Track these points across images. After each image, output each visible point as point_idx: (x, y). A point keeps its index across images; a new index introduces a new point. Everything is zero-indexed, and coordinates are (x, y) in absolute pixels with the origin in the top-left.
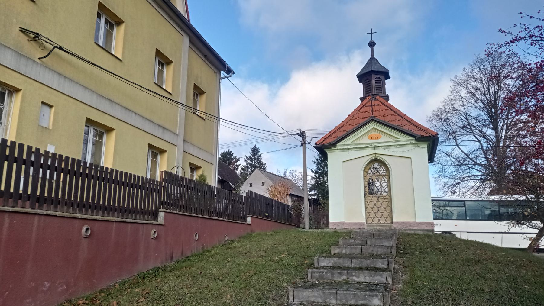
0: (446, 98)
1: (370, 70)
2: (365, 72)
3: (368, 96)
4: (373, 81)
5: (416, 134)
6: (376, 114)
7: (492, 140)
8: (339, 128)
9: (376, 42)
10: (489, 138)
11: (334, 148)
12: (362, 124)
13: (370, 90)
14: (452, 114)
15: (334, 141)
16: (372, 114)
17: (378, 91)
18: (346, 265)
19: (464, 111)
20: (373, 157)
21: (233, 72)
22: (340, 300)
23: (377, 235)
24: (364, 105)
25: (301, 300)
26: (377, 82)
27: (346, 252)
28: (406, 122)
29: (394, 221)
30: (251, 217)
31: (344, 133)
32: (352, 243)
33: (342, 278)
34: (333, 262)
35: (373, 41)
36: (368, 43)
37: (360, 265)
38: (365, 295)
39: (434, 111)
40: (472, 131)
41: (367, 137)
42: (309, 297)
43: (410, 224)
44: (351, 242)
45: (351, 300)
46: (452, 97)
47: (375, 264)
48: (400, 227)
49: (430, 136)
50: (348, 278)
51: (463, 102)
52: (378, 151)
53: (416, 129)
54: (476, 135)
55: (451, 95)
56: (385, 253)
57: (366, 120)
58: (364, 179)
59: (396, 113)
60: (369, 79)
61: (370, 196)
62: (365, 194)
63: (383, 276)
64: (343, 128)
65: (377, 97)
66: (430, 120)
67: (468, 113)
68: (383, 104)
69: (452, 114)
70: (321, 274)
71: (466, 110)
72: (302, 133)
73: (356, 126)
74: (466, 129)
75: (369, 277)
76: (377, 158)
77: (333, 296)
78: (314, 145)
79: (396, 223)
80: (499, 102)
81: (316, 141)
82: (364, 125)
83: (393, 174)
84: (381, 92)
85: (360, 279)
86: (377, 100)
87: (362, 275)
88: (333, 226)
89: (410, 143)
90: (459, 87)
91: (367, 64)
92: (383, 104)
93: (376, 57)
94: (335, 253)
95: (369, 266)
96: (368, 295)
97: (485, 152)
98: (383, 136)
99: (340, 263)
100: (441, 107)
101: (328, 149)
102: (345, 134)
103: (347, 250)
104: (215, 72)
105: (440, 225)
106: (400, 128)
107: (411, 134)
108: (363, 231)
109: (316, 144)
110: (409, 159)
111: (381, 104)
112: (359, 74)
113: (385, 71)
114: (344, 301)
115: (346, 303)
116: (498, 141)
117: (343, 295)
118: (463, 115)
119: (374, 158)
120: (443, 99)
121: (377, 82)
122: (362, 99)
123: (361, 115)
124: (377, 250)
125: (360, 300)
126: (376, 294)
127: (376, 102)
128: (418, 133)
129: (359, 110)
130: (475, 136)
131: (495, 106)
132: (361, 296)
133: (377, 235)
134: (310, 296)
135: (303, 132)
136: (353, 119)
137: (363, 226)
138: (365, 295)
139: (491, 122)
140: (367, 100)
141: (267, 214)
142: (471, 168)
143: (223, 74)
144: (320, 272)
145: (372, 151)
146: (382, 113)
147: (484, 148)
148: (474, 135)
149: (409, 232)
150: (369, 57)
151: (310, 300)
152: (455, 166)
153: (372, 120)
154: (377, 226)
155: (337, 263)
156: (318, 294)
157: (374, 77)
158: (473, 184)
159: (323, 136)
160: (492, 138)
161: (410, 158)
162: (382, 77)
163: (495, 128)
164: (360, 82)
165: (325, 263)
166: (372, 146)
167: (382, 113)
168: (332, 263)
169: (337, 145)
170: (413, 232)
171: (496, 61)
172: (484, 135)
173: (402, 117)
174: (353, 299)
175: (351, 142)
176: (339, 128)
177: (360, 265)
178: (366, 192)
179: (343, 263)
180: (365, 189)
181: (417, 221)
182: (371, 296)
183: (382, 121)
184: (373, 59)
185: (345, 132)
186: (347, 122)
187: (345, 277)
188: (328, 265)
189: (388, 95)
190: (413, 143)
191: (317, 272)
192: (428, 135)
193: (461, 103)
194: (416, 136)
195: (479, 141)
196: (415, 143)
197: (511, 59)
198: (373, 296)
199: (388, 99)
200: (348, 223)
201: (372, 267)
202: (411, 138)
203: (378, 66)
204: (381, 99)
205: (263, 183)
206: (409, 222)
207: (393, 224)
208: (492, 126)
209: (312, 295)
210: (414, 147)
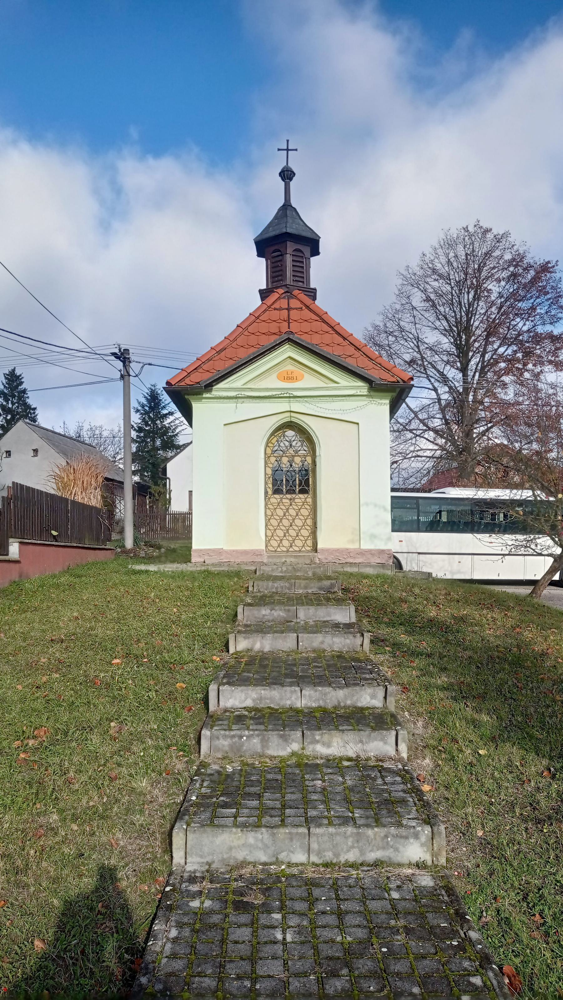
0: (388, 307)
1: (284, 230)
2: (272, 234)
3: (277, 288)
4: (288, 256)
5: (372, 376)
6: (294, 327)
7: (456, 388)
8: (219, 350)
9: (295, 171)
10: (452, 385)
11: (208, 395)
12: (267, 347)
13: (281, 275)
14: (396, 337)
15: (208, 380)
16: (289, 328)
17: (297, 279)
18: (288, 702)
19: (415, 333)
20: (285, 418)
22: (319, 853)
23: (302, 585)
24: (269, 307)
25: (209, 859)
26: (295, 259)
27: (262, 646)
28: (352, 350)
29: (319, 546)
30: (20, 543)
31: (229, 365)
32: (266, 617)
33: (289, 750)
34: (254, 695)
35: (291, 169)
36: (279, 171)
37: (322, 703)
38: (386, 836)
39: (367, 329)
40: (425, 369)
41: (275, 376)
42: (231, 849)
43: (349, 553)
44: (264, 615)
45: (348, 851)
46: (398, 307)
47: (355, 698)
48: (331, 558)
49: (398, 382)
50: (303, 749)
51: (414, 317)
52: (296, 406)
53: (370, 364)
54: (433, 380)
55: (396, 301)
56: (349, 648)
57: (273, 339)
58: (266, 463)
59: (332, 327)
60: (279, 251)
61: (276, 496)
62: (266, 493)
63: (389, 741)
64: (229, 353)
65: (296, 292)
67: (420, 337)
68: (307, 307)
69: (396, 337)
70: (237, 739)
71: (418, 331)
72: (122, 354)
73: (252, 350)
74: (415, 366)
75: (356, 743)
76: (293, 420)
77: (298, 844)
78: (165, 386)
79: (323, 550)
80: (474, 321)
81: (168, 378)
83: (322, 455)
84: (303, 282)
85: (333, 748)
86: (296, 297)
87: (340, 740)
88: (200, 556)
89: (359, 393)
90: (410, 288)
91: (276, 217)
92: (307, 307)
93: (294, 203)
94: (238, 649)
95: (342, 704)
96: (393, 836)
97: (442, 410)
98: (306, 375)
99: (272, 699)
100: (378, 323)
101: (194, 395)
102: (232, 366)
103: (264, 641)
106: (342, 360)
107: (363, 374)
108: (263, 570)
109: (168, 383)
110: (356, 425)
111: (304, 308)
112: (258, 239)
113: (315, 237)
114: (329, 856)
115: (334, 861)
116: (466, 391)
117: (326, 838)
118: (413, 340)
119: (288, 420)
120: (381, 309)
121: (295, 259)
122: (264, 294)
123: (264, 327)
124: (331, 642)
125: (371, 851)
126: (414, 833)
127: (294, 303)
128: (376, 374)
129: (259, 316)
130: (430, 381)
131: (467, 329)
132: (375, 839)
133: (302, 585)
134: (235, 847)
135: (124, 350)
136: (246, 333)
137: (259, 557)
138: (386, 836)
139: (458, 356)
140: (274, 297)
141: (54, 533)
142: (419, 436)
144: (233, 736)
145: (283, 406)
146: (306, 327)
147: (443, 403)
148: (428, 377)
149: (349, 569)
150: (282, 202)
151: (235, 858)
152: (394, 431)
153: (289, 340)
154: (286, 557)
155: (265, 698)
156: (256, 839)
157: (291, 247)
158: (420, 465)
159: (184, 366)
160: (457, 385)
161: (358, 424)
162: (307, 250)
163: (464, 370)
164: (260, 254)
165: (235, 699)
166: (285, 395)
167: (306, 327)
168: (254, 700)
169: (214, 388)
170: (355, 570)
171: (476, 245)
172: (445, 380)
173: (345, 339)
174: (353, 847)
175: (244, 385)
176: (219, 352)
177: (321, 702)
178: (268, 490)
179: (281, 699)
180: (266, 483)
181: (363, 547)
182: (401, 837)
183: (308, 344)
184: (289, 207)
185: (231, 362)
186: (235, 339)
187: (295, 747)
188: (244, 705)
189: (315, 289)
190: (365, 393)
191: (225, 737)
192: (394, 380)
193: (412, 319)
194: (372, 379)
195: (435, 390)
197: (501, 244)
198: (406, 838)
199: (314, 298)
200: (230, 551)
201: (349, 707)
202: (360, 383)
203: (299, 224)
204: (302, 296)
205: (36, 451)
207: (316, 552)
208: (459, 364)
209: (242, 842)
210: (366, 402)
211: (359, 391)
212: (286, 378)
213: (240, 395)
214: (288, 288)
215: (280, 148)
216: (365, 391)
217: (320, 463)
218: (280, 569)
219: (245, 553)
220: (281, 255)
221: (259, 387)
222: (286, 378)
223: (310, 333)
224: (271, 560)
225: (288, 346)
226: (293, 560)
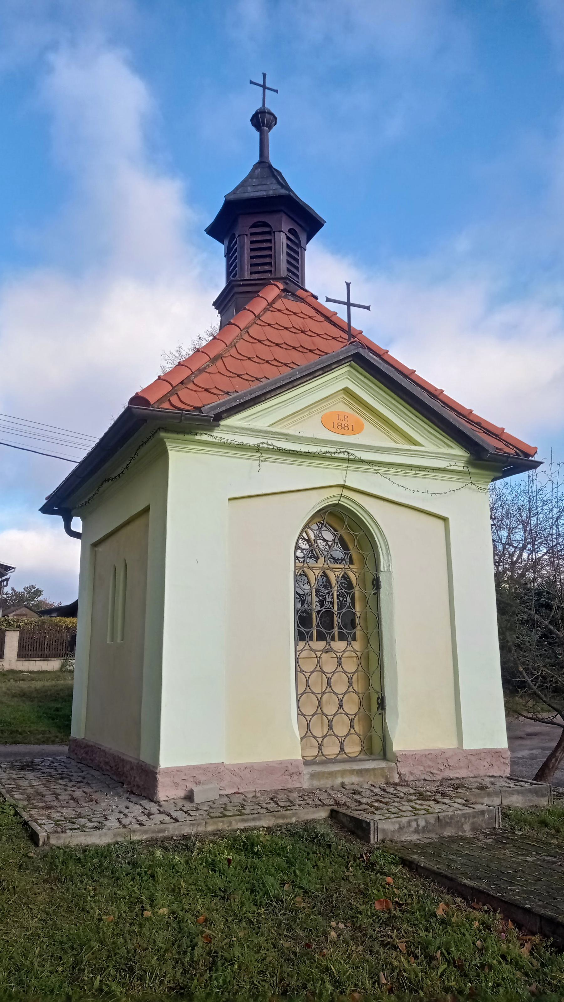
11: (205, 438)
48: (418, 772)
49: (518, 454)
76: (344, 502)
82: (327, 369)
83: (394, 569)
88: (176, 785)
98: (367, 426)
101: (178, 432)
108: (384, 830)
112: (232, 197)
150: (257, 159)
154: (343, 773)
161: (445, 519)
166: (342, 455)
169: (222, 423)
181: (467, 746)
190: (461, 469)
202: (458, 451)
206: (443, 752)
211: (452, 464)
212: (336, 425)
213: (265, 445)
215: (254, 80)
216: (460, 466)
217: (390, 585)
218: (414, 824)
220: (269, 233)
221: (301, 435)
222: (336, 425)
223: (246, 377)
224: (316, 783)
226: (355, 779)
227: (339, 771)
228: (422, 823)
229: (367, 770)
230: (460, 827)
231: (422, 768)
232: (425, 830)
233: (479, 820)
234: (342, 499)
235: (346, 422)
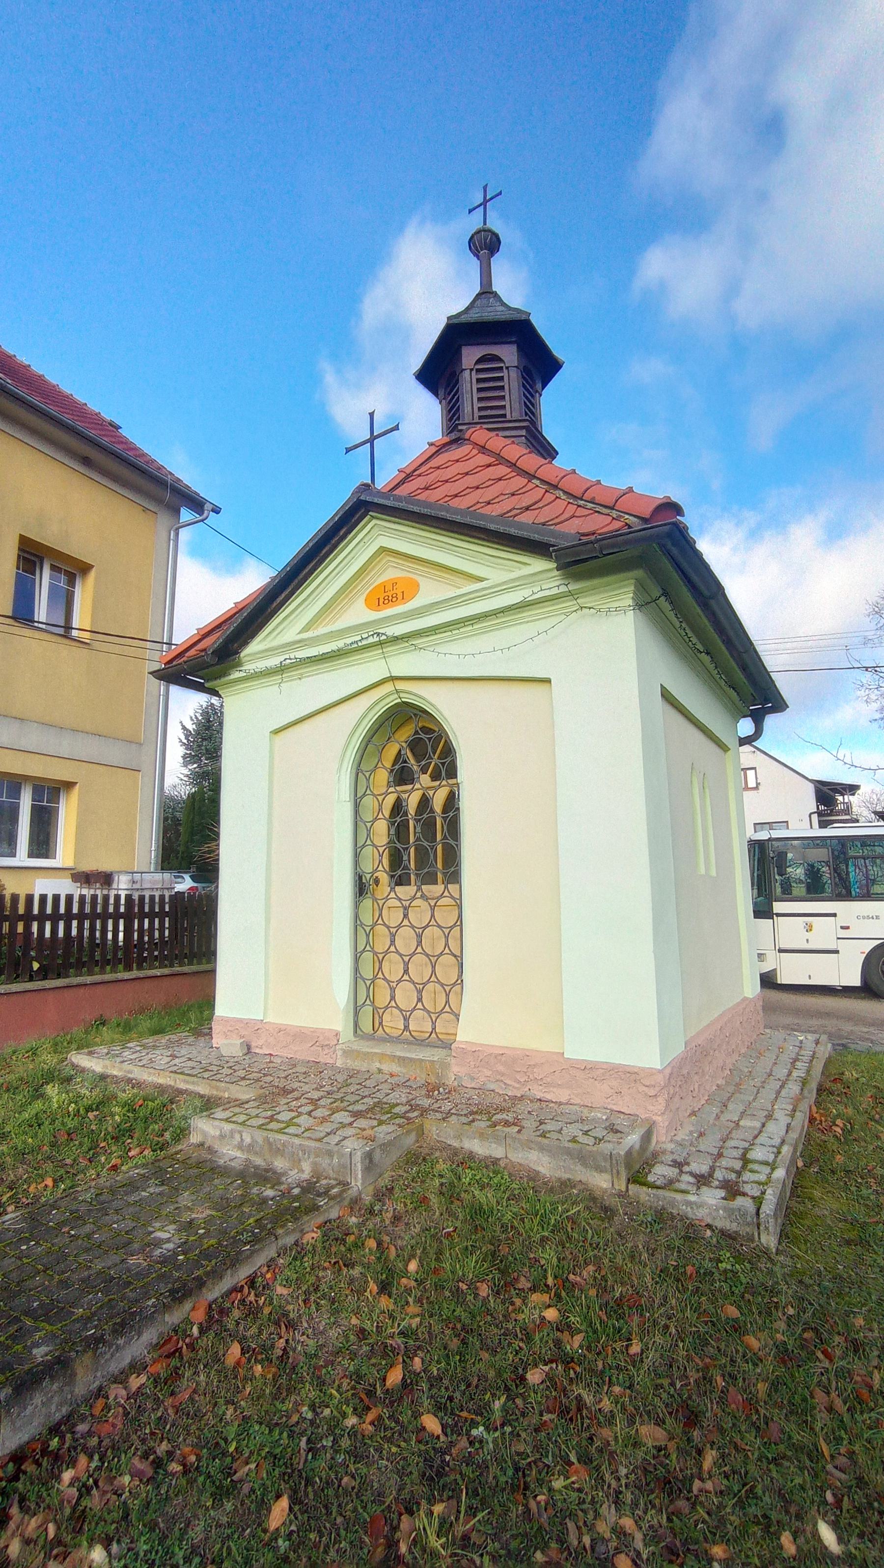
4: (466, 374)
11: (236, 675)
21: (208, 506)
48: (484, 1076)
66: (876, 609)
104: (145, 509)
105: (877, 917)
119: (394, 700)
143: (186, 515)
161: (548, 681)
169: (242, 655)
190: (555, 591)
192: (617, 525)
196: (563, 589)
202: (538, 565)
206: (527, 1054)
213: (288, 661)
214: (461, 431)
219: (300, 1035)
224: (351, 1064)
225: (374, 522)
227: (376, 1053)
228: (248, 1139)
229: (411, 1059)
230: (296, 1162)
231: (489, 1073)
232: (250, 1148)
233: (324, 1162)
234: (402, 695)
235: (395, 591)
